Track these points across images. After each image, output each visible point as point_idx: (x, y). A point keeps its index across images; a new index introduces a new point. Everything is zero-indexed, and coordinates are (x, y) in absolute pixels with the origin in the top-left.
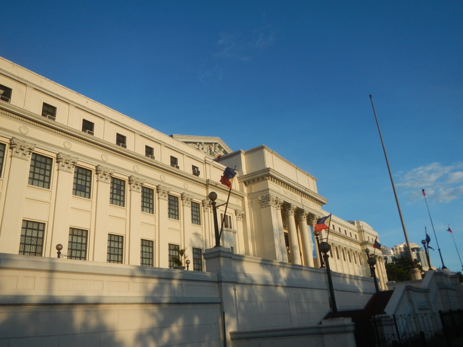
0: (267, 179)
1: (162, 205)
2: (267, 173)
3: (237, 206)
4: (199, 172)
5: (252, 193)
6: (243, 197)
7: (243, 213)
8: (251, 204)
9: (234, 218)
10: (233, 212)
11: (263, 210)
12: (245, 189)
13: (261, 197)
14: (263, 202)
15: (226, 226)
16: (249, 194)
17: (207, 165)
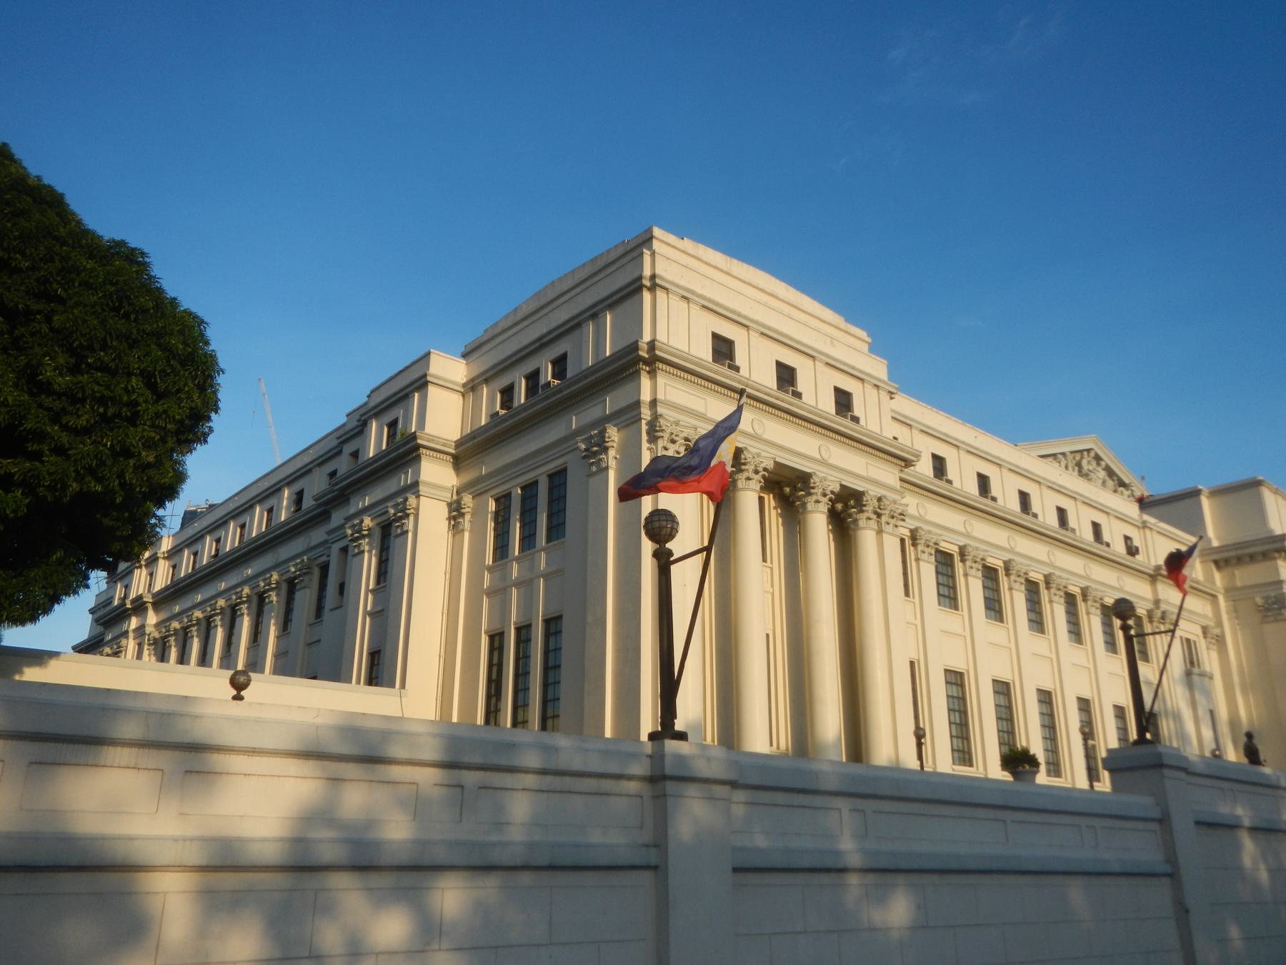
0: (1275, 559)
1: (1056, 613)
2: (1277, 545)
3: (1205, 616)
4: (1137, 549)
5: (1236, 589)
6: (1214, 596)
7: (1217, 631)
8: (1235, 611)
9: (1202, 644)
10: (1199, 631)
11: (1270, 628)
12: (1217, 576)
13: (1266, 598)
14: (1268, 610)
15: (1192, 663)
16: (1230, 590)
17: (1147, 531)
